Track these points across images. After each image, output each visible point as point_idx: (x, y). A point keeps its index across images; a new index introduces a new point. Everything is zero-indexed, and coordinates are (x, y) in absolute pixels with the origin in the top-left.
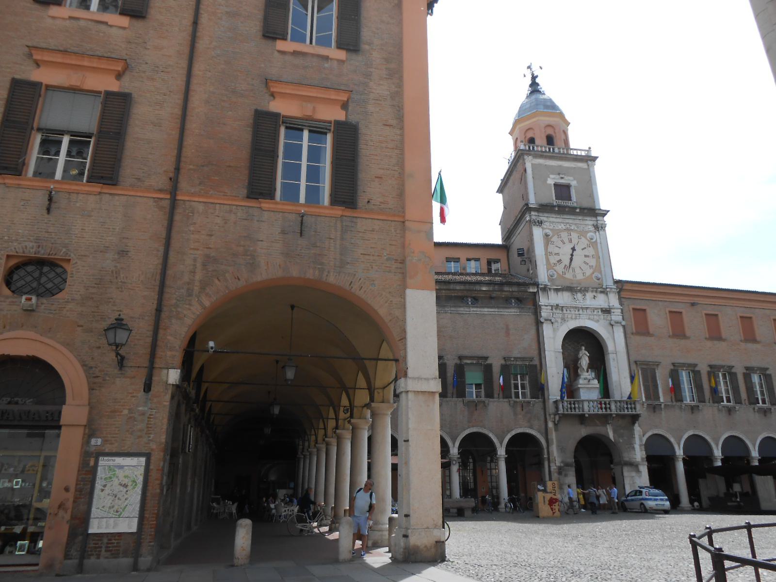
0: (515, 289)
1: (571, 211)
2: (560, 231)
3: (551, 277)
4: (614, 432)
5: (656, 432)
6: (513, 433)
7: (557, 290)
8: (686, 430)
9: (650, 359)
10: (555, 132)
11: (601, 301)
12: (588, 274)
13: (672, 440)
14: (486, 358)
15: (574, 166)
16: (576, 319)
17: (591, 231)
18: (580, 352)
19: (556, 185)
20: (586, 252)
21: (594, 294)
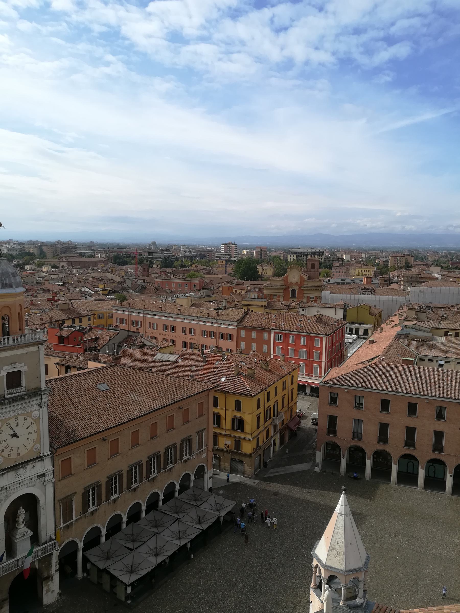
1: (21, 398)
2: (10, 418)
8: (87, 529)
10: (11, 313)
11: (39, 468)
15: (26, 352)
16: (17, 491)
17: (35, 410)
18: (19, 512)
20: (29, 430)
21: (34, 464)
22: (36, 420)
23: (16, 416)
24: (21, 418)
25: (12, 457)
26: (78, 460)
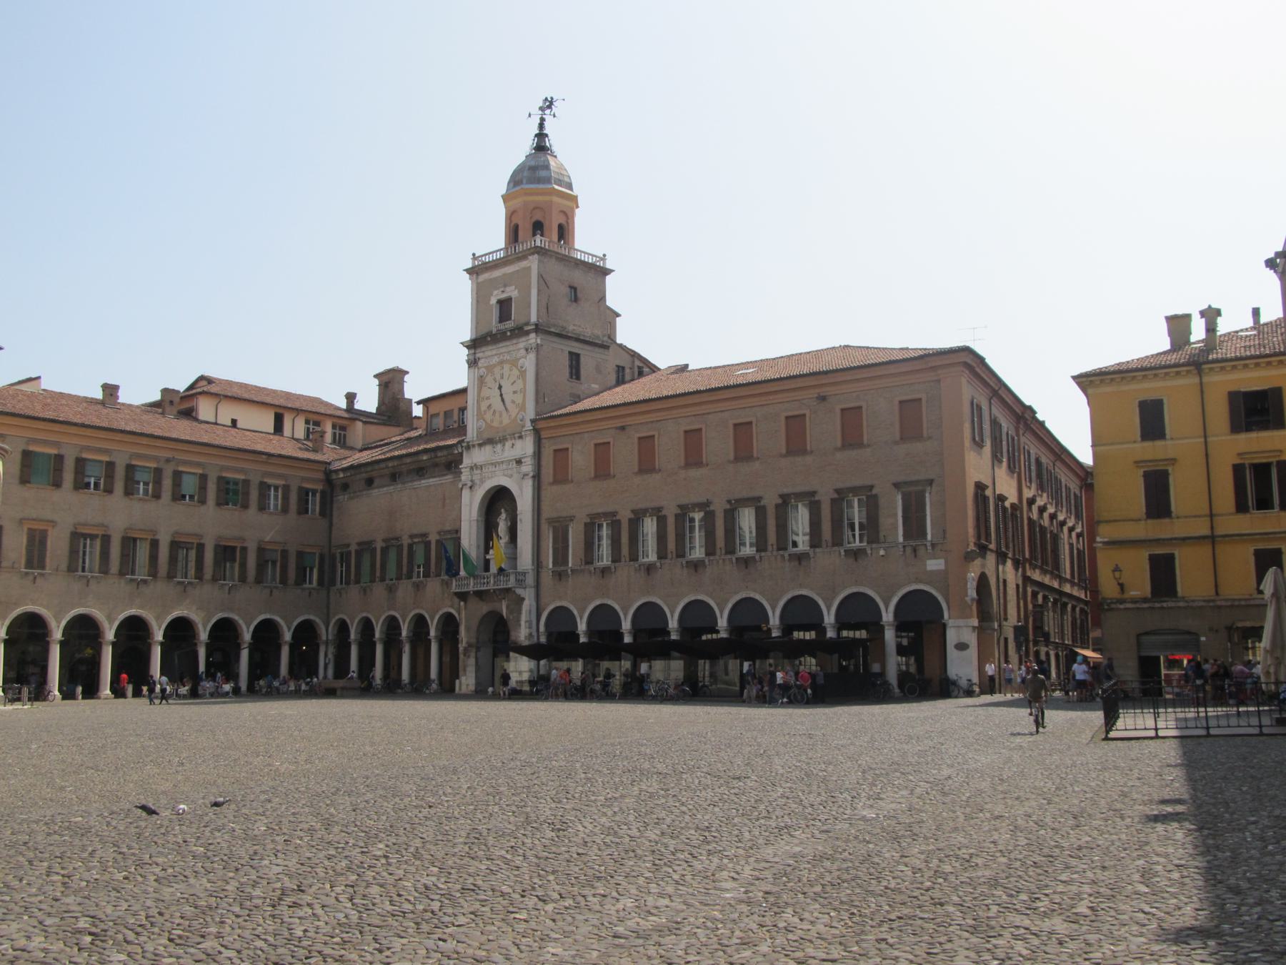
0: (445, 453)
2: (495, 366)
3: (479, 428)
4: (508, 607)
5: (558, 604)
6: (441, 613)
7: (480, 445)
9: (564, 514)
12: (513, 415)
13: (575, 612)
14: (425, 535)
19: (500, 302)
22: (523, 374)
23: (501, 363)
24: (507, 367)
25: (495, 424)
26: (581, 459)
